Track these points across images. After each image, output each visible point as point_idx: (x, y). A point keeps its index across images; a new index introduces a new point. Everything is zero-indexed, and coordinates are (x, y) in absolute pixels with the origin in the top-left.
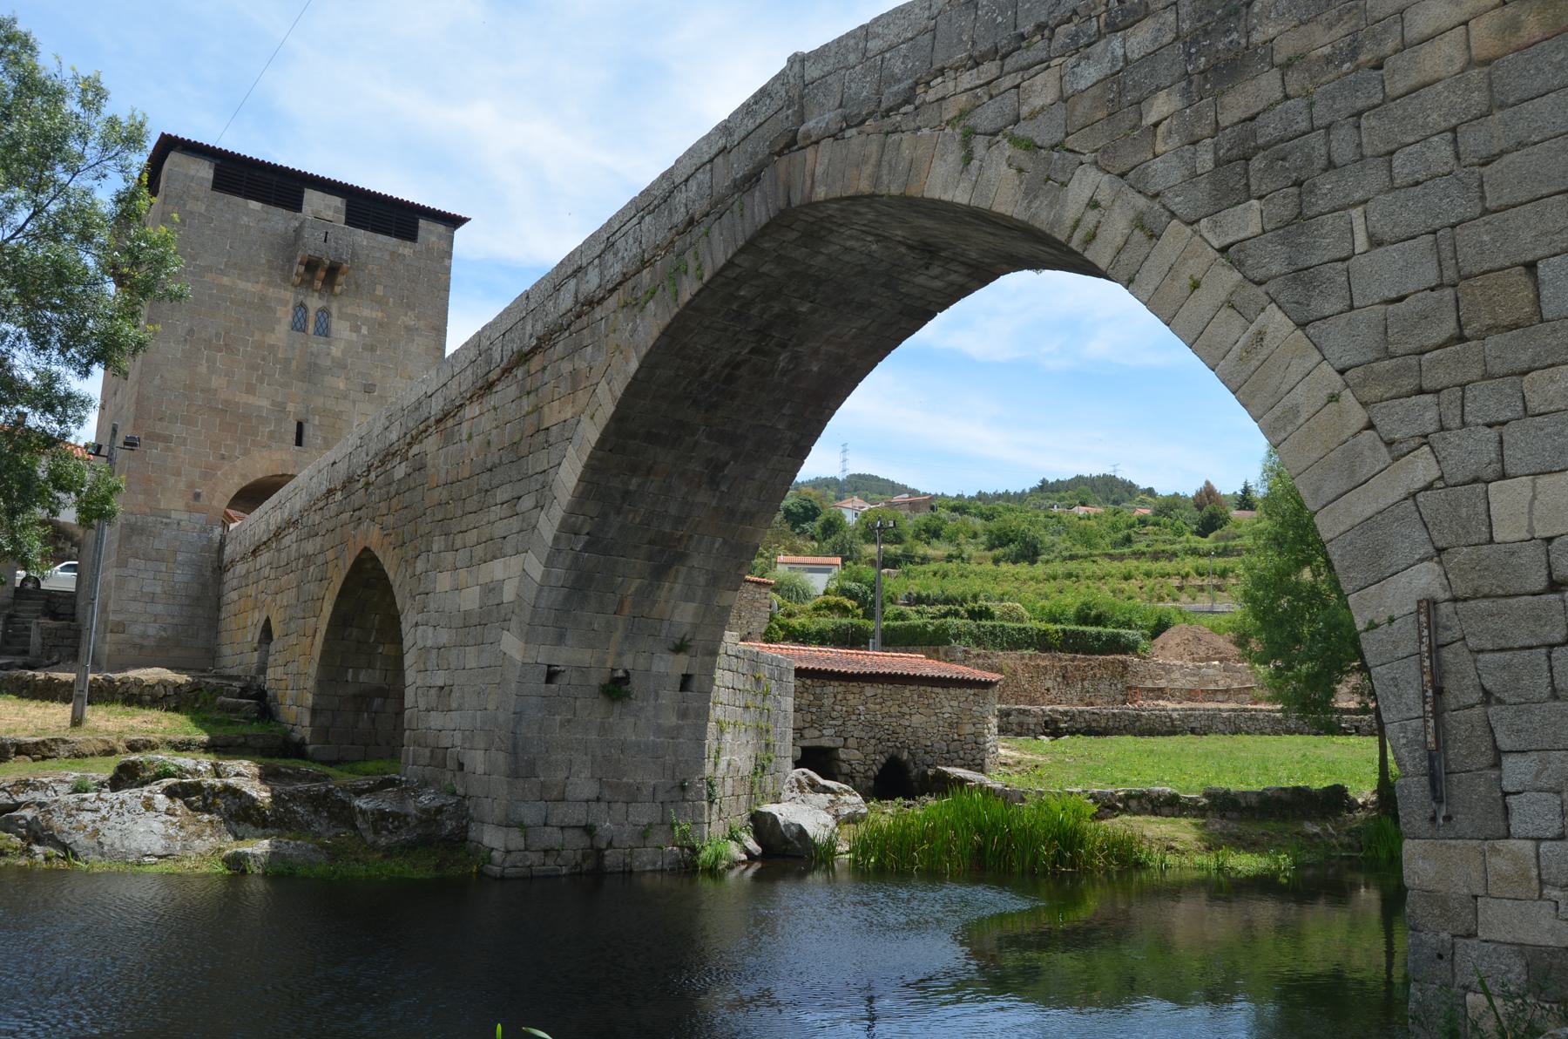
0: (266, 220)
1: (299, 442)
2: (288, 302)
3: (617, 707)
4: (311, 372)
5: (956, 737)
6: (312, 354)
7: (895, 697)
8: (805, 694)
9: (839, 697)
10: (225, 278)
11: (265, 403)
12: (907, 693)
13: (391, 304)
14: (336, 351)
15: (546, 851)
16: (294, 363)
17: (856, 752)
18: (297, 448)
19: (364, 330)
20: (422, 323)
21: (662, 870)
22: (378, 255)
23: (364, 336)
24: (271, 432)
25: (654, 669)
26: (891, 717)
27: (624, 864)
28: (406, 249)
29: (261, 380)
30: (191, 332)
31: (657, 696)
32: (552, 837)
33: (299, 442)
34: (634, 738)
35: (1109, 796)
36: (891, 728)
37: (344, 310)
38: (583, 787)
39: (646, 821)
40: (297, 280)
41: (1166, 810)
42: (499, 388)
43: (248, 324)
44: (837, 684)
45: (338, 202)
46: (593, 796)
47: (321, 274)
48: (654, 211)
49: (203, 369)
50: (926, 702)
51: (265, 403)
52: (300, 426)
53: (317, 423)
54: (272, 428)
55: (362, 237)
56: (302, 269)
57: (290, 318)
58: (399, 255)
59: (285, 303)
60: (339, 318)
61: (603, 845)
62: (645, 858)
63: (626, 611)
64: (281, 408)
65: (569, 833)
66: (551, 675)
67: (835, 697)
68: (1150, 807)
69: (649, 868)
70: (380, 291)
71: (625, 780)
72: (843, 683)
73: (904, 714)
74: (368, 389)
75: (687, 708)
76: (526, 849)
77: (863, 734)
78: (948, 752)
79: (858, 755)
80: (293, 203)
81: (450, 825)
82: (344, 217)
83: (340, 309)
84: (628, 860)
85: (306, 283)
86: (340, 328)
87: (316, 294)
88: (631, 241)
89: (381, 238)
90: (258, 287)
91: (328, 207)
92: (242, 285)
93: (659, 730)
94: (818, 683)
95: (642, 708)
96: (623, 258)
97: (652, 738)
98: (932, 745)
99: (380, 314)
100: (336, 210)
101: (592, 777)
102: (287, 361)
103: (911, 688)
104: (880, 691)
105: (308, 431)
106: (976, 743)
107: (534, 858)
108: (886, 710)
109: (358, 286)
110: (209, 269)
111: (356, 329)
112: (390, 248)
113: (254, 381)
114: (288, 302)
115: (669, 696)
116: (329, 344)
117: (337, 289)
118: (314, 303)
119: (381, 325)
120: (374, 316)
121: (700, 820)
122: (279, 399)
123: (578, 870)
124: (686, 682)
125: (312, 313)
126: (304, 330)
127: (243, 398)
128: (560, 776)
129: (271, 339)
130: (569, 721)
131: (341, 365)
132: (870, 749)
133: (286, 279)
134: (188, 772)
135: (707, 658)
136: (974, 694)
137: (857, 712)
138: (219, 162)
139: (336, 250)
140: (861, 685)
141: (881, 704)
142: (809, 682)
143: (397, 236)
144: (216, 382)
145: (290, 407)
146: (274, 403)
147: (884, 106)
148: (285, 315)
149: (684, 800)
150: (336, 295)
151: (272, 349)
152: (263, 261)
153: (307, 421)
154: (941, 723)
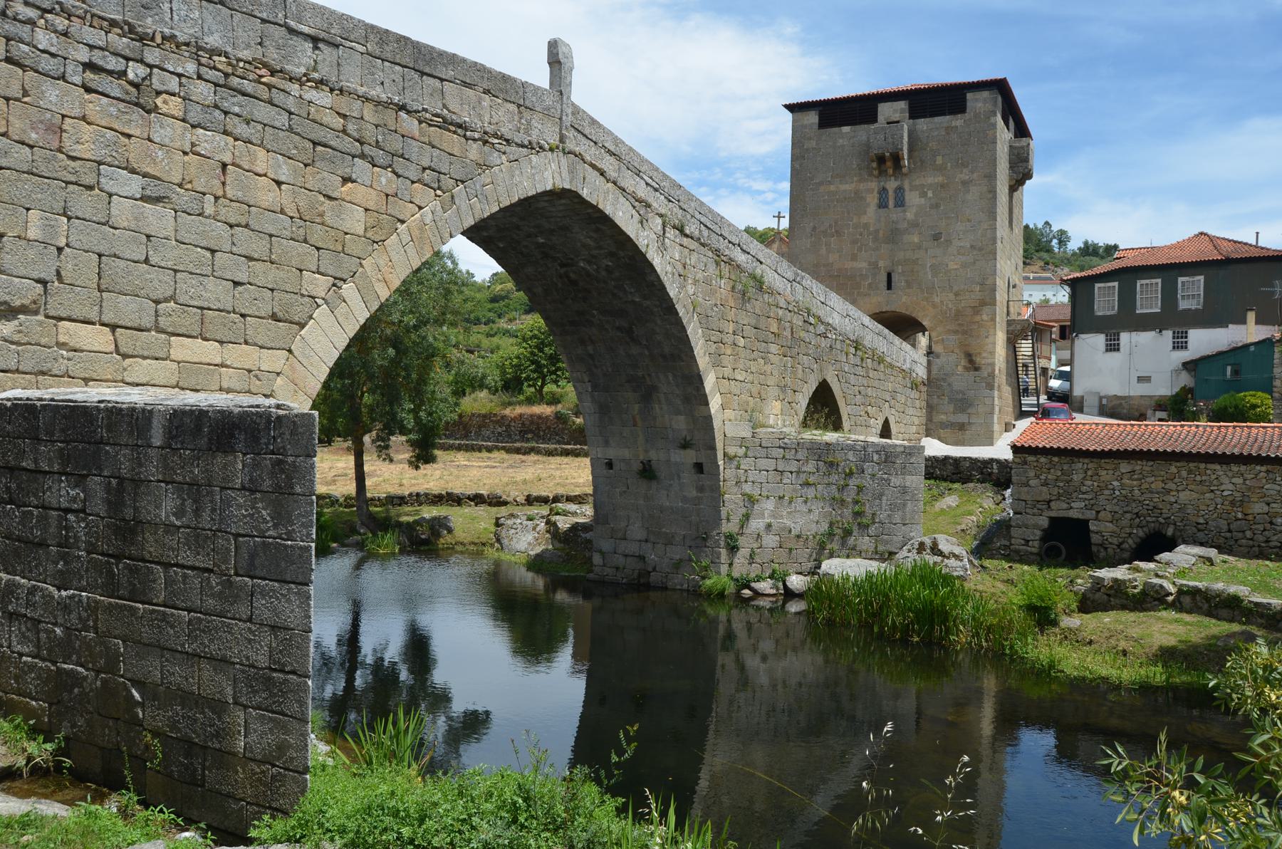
0: (854, 137)
1: (889, 287)
2: (873, 190)
3: (654, 484)
4: (894, 236)
5: (1240, 515)
6: (893, 222)
7: (1156, 473)
8: (1052, 471)
9: (1089, 473)
11: (864, 265)
12: (1173, 469)
14: (910, 215)
15: (617, 568)
16: (881, 232)
17: (1111, 525)
18: (887, 292)
19: (930, 194)
20: (975, 175)
21: (688, 590)
22: (936, 133)
23: (930, 198)
24: (870, 284)
25: (672, 459)
27: (662, 583)
28: (957, 121)
29: (860, 249)
30: (814, 228)
31: (679, 477)
32: (620, 561)
33: (889, 287)
34: (668, 504)
35: (1157, 588)
36: (1152, 504)
37: (914, 183)
38: (636, 531)
39: (678, 557)
40: (876, 173)
41: (1224, 612)
43: (849, 213)
44: (1086, 461)
45: (903, 105)
46: (643, 538)
47: (889, 164)
49: (823, 251)
50: (1198, 478)
51: (864, 265)
52: (889, 276)
53: (900, 271)
55: (923, 124)
56: (874, 165)
57: (876, 201)
59: (871, 191)
60: (911, 190)
61: (650, 569)
62: (676, 581)
63: (639, 423)
64: (874, 266)
65: (630, 559)
66: (610, 465)
67: (1086, 472)
68: (1206, 606)
69: (678, 587)
70: (939, 160)
71: (664, 530)
72: (1095, 460)
73: (1168, 492)
74: (936, 237)
75: (703, 485)
76: (604, 565)
77: (1116, 508)
78: (1230, 531)
79: (1110, 526)
80: (873, 118)
83: (910, 183)
84: (664, 580)
85: (882, 173)
86: (913, 198)
87: (893, 178)
89: (937, 119)
90: (853, 185)
91: (895, 111)
93: (685, 499)
94: (1064, 459)
95: (671, 485)
97: (680, 504)
98: (1207, 523)
99: (941, 179)
100: (902, 111)
101: (643, 526)
102: (877, 231)
103: (1178, 464)
104: (1138, 468)
105: (895, 278)
106: (1271, 523)
107: (608, 571)
108: (1145, 486)
109: (922, 162)
110: (821, 183)
111: (924, 195)
112: (945, 125)
114: (873, 190)
115: (688, 477)
116: (905, 211)
117: (904, 170)
118: (892, 185)
119: (942, 186)
120: (936, 181)
121: (717, 561)
123: (636, 582)
124: (699, 467)
125: (891, 193)
126: (886, 206)
127: (849, 265)
128: (623, 524)
129: (864, 219)
130: (625, 492)
131: (914, 225)
132: (1125, 522)
133: (871, 175)
134: (570, 513)
135: (709, 452)
136: (1268, 472)
137: (1111, 487)
138: (821, 108)
139: (893, 143)
140: (1116, 461)
141: (1140, 480)
142: (1056, 459)
143: (950, 113)
144: (832, 258)
145: (881, 264)
148: (873, 200)
149: (706, 546)
150: (906, 175)
151: (866, 226)
152: (855, 166)
153: (893, 271)
154: (1219, 500)
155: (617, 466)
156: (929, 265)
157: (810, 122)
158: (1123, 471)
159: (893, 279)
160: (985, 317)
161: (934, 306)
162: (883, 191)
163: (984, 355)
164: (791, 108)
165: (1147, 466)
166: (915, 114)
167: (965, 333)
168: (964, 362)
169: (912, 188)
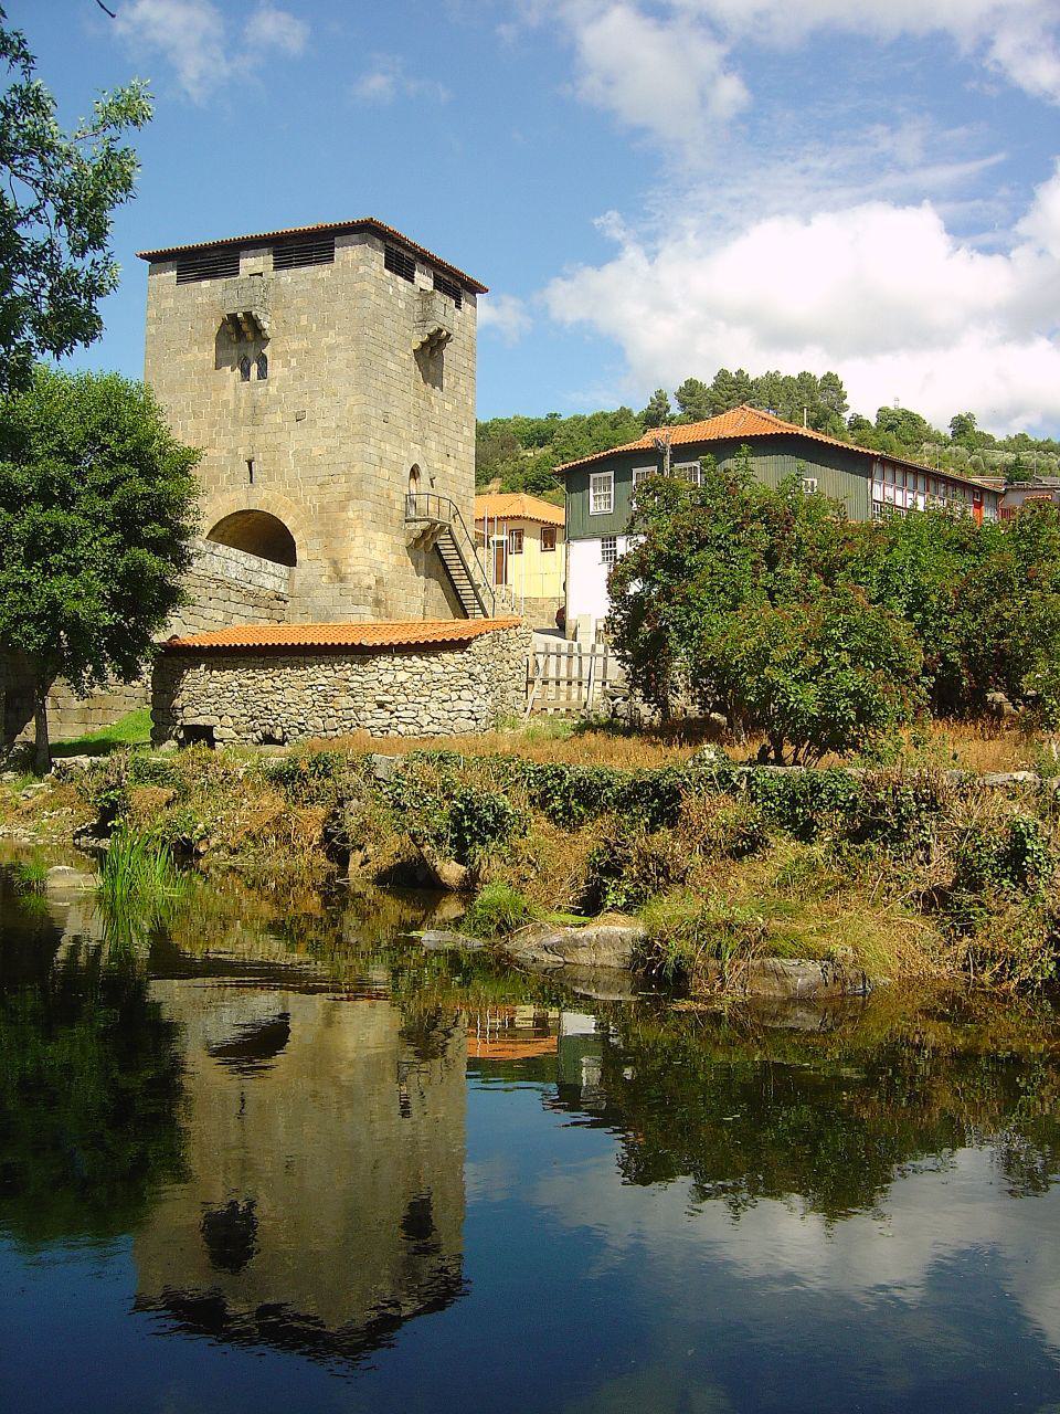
4: (256, 415)
14: (272, 390)
19: (294, 363)
40: (234, 338)
55: (288, 276)
86: (275, 369)
89: (304, 270)
111: (287, 364)
151: (226, 404)
156: (291, 452)
160: (351, 514)
161: (297, 502)
163: (351, 561)
164: (143, 257)
167: (329, 535)
168: (329, 571)
169: (276, 355)
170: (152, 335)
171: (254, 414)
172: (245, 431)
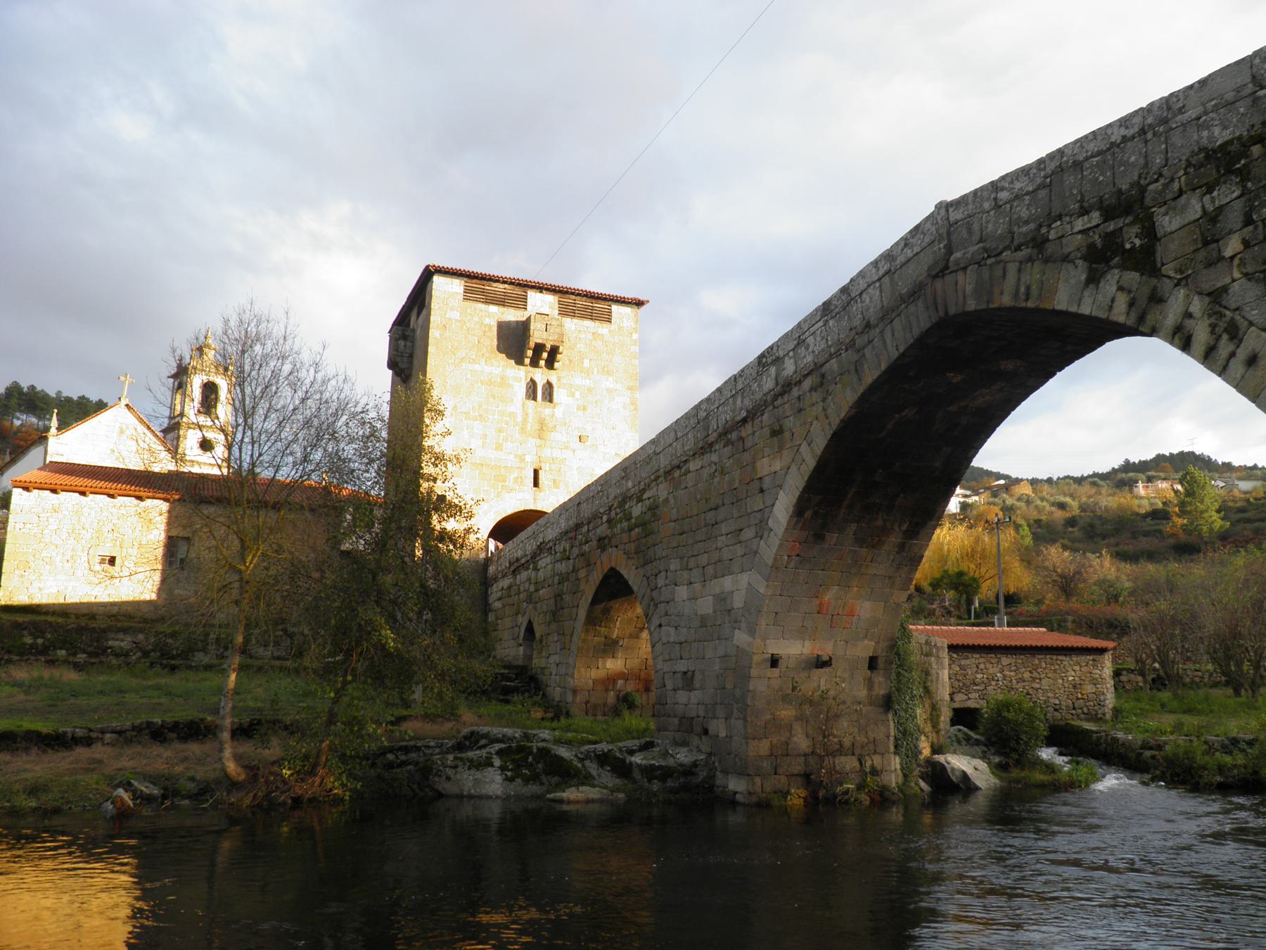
1: (536, 484)
4: (542, 429)
5: (1079, 696)
10: (476, 366)
12: (1037, 662)
13: (595, 373)
23: (577, 399)
26: (1024, 681)
33: (536, 484)
42: (717, 447)
44: (978, 656)
47: (545, 355)
48: (836, 316)
52: (536, 472)
53: (548, 469)
54: (516, 475)
55: (571, 324)
58: (599, 335)
70: (586, 363)
72: (983, 655)
78: (1074, 709)
80: (522, 303)
81: (702, 774)
82: (557, 312)
85: (534, 363)
88: (818, 339)
90: (500, 369)
92: (487, 369)
96: (813, 352)
99: (588, 381)
103: (1040, 657)
105: (541, 475)
112: (593, 330)
113: (501, 441)
119: (590, 390)
122: (519, 453)
126: (535, 399)
136: (1093, 660)
137: (996, 678)
138: (465, 279)
145: (528, 458)
146: (516, 456)
147: (1016, 243)
148: (521, 389)
151: (512, 415)
155: (782, 664)
156: (575, 468)
157: (454, 290)
158: (1004, 664)
159: (540, 477)
162: (532, 385)
165: (1020, 659)
166: (565, 311)
170: (436, 338)
171: (541, 429)
172: (533, 442)
